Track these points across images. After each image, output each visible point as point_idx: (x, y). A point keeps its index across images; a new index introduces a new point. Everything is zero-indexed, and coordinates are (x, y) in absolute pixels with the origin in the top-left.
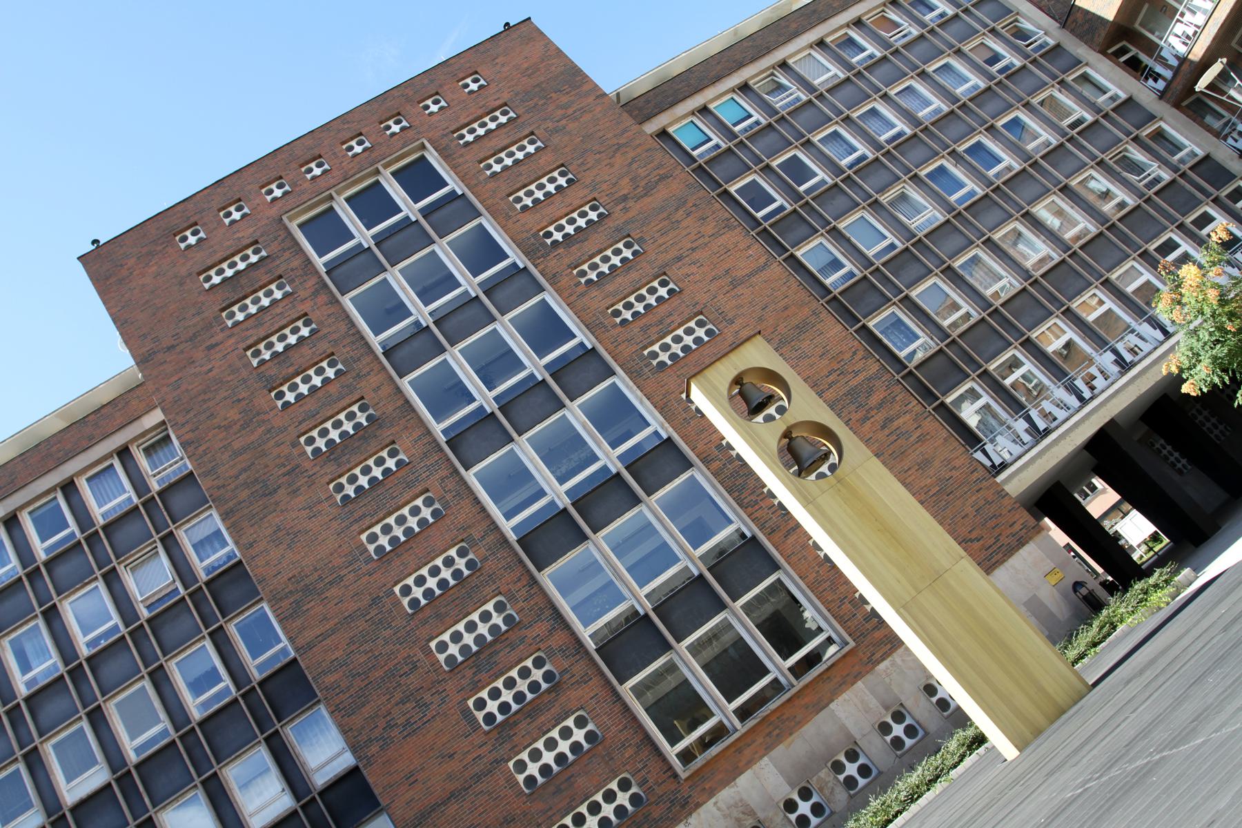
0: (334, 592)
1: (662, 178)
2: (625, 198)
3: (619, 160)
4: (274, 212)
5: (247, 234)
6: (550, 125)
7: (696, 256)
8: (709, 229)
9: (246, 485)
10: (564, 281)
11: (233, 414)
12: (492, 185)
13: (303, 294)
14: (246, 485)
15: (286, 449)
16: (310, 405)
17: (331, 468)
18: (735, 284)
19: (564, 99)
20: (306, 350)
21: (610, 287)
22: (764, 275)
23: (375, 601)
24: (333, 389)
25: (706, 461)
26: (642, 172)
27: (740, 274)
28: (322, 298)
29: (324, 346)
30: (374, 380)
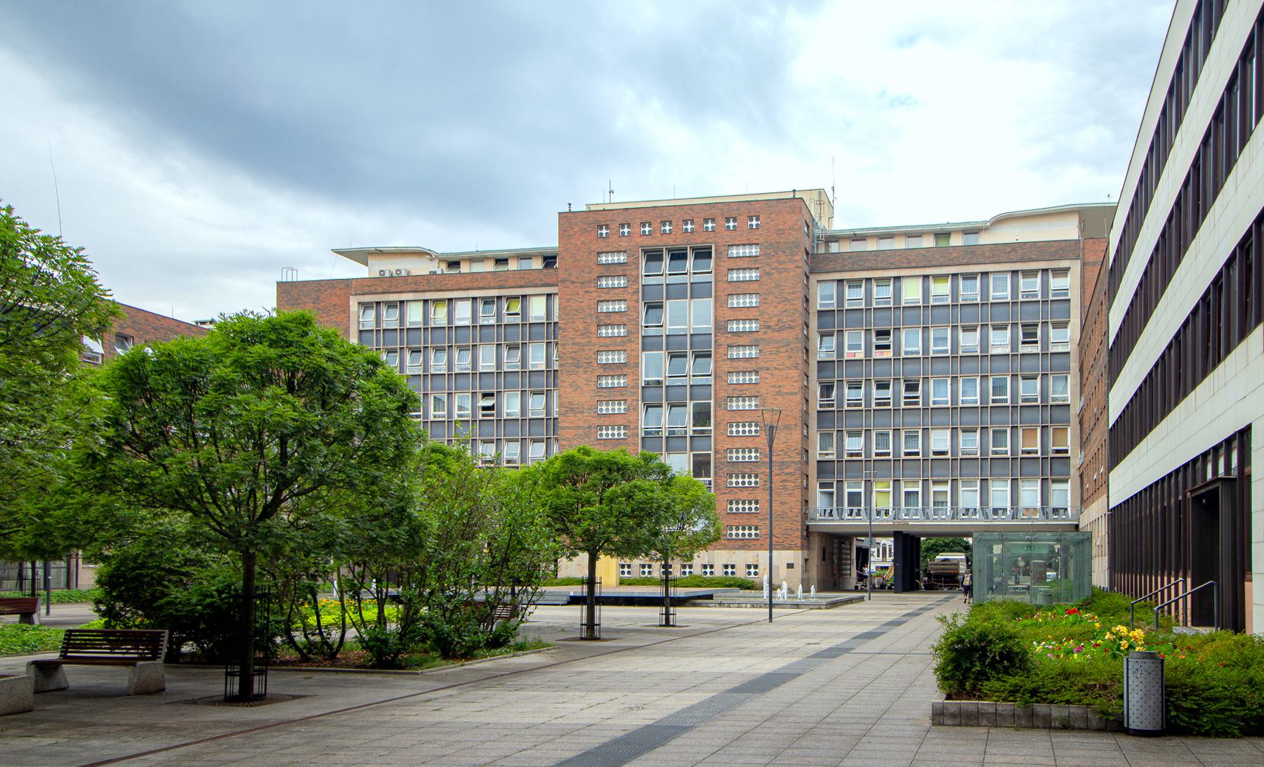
0: (579, 416)
1: (791, 327)
2: (769, 327)
3: (780, 307)
4: (640, 241)
5: (624, 244)
6: (768, 269)
7: (776, 372)
8: (788, 363)
9: (573, 358)
10: (722, 350)
11: (581, 327)
12: (726, 285)
13: (630, 290)
14: (573, 358)
15: (591, 354)
16: (608, 341)
17: (601, 372)
18: (778, 393)
19: (783, 259)
20: (618, 316)
21: (735, 364)
22: (791, 397)
23: (590, 427)
24: (618, 340)
25: (716, 452)
26: (785, 319)
27: (784, 390)
28: (635, 297)
29: (624, 319)
30: (634, 346)
